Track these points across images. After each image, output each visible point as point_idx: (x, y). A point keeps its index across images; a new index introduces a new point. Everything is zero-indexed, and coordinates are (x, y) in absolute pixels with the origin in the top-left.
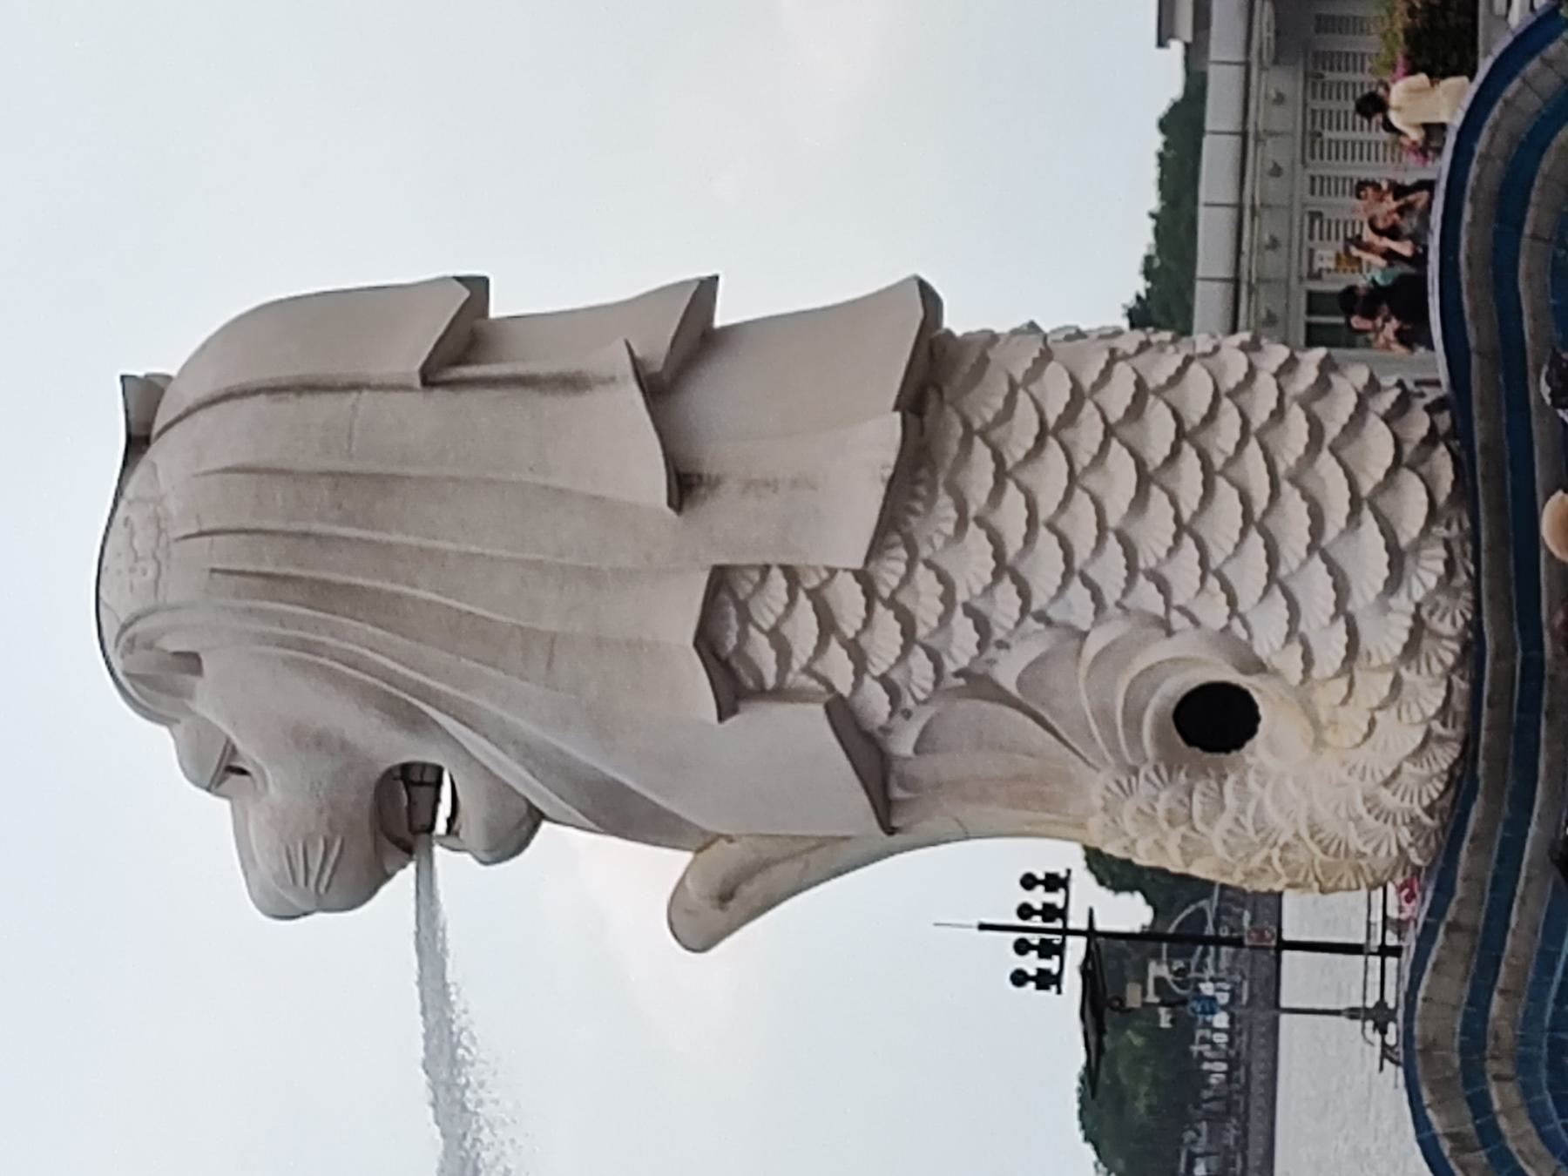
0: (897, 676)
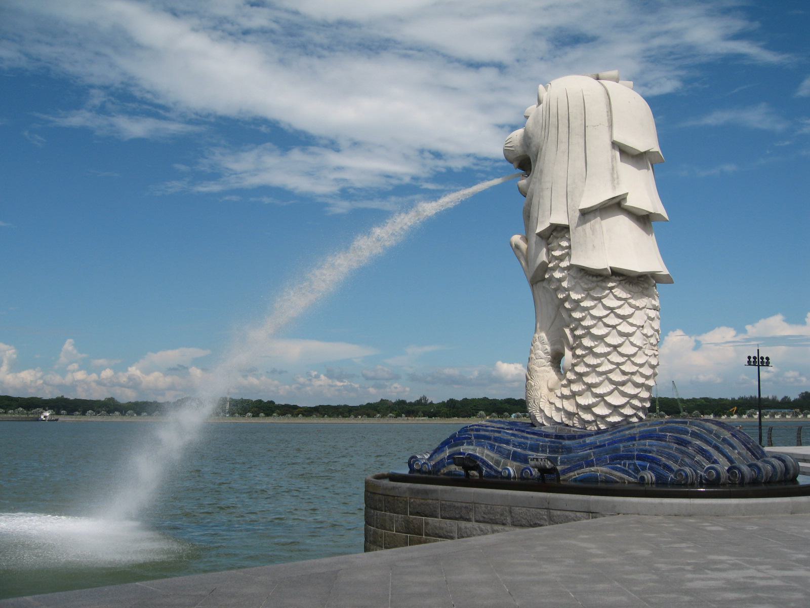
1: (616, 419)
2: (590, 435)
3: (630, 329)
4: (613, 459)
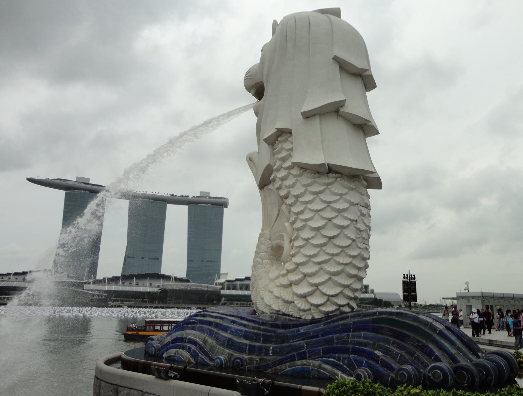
0: (277, 179)
1: (330, 308)
2: (303, 325)
3: (346, 223)
4: (327, 352)
